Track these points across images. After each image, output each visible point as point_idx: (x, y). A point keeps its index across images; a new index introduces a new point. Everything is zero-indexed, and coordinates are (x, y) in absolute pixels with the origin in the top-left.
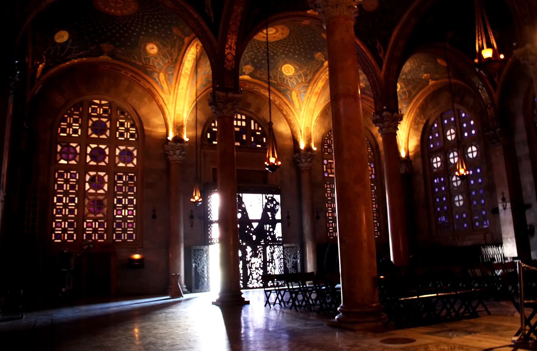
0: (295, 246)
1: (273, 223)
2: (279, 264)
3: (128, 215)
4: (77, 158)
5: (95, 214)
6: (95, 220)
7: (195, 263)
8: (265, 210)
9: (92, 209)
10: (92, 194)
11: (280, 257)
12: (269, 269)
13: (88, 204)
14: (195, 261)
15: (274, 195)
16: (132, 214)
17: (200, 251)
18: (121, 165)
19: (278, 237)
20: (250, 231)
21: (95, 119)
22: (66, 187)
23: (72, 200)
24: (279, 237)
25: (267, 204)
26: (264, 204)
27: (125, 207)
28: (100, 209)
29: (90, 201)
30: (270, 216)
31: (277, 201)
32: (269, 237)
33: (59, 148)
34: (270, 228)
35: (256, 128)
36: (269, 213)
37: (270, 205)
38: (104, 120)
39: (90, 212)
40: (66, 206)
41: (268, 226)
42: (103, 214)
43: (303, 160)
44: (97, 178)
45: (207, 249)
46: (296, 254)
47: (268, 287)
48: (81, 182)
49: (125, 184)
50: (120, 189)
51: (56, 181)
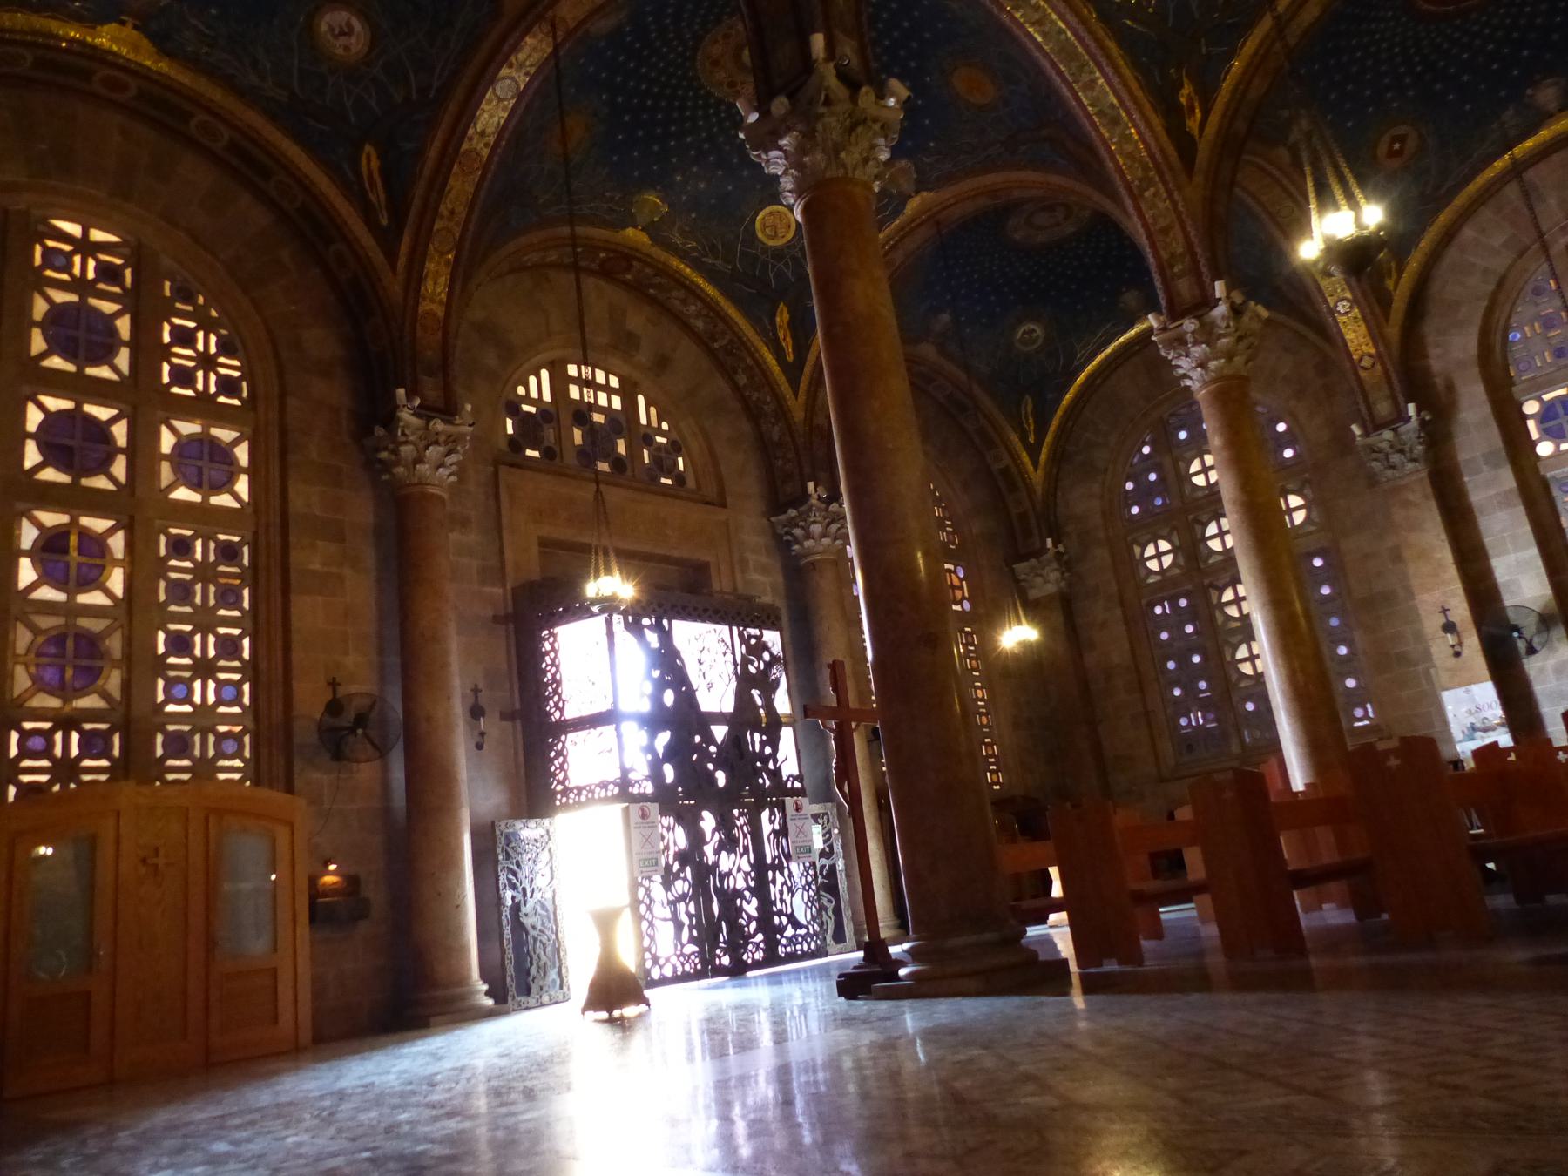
1: (773, 727)
2: (802, 874)
6: (67, 723)
7: (514, 887)
10: (48, 607)
12: (774, 891)
13: (28, 650)
14: (509, 880)
15: (765, 632)
16: (237, 701)
18: (183, 494)
20: (706, 756)
21: (60, 297)
25: (746, 662)
27: (204, 669)
28: (90, 678)
29: (41, 639)
30: (759, 702)
34: (763, 744)
35: (654, 424)
36: (755, 693)
37: (756, 664)
39: (39, 685)
41: (757, 737)
42: (105, 696)
43: (816, 529)
44: (74, 540)
45: (548, 831)
49: (204, 572)
50: (181, 592)
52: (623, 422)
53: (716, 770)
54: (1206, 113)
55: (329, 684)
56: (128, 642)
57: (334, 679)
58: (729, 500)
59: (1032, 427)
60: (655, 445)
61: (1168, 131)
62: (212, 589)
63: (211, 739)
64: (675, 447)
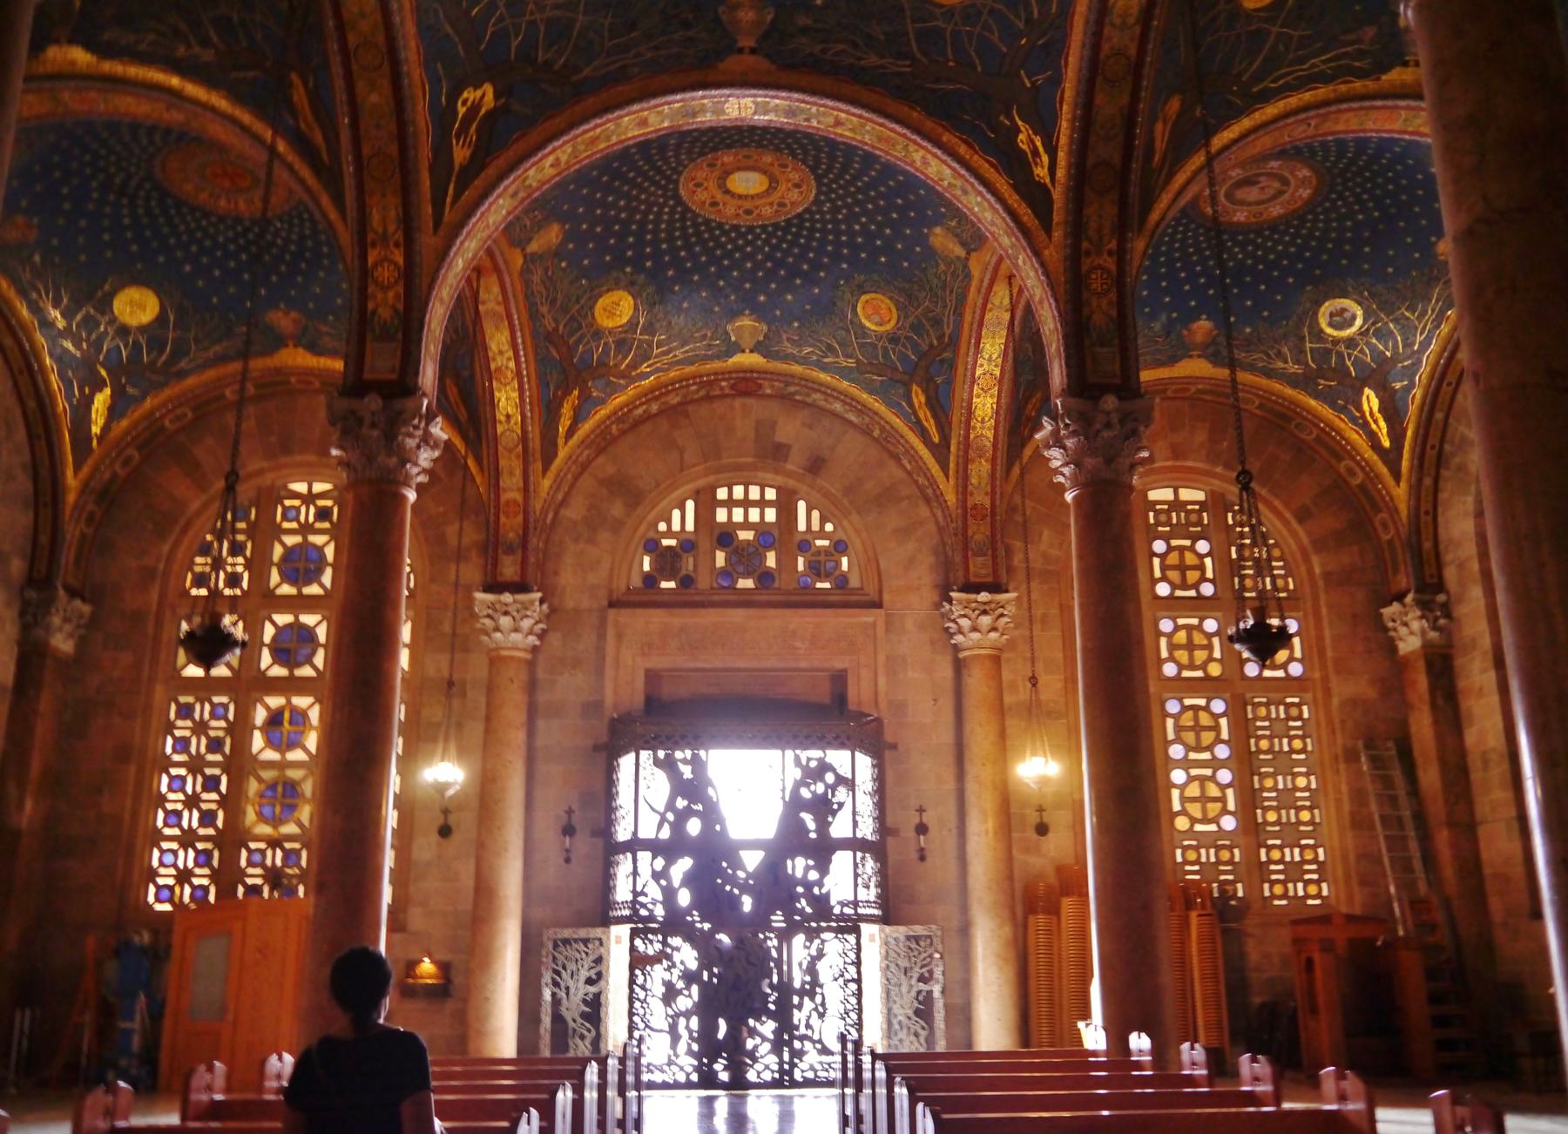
0: (926, 933)
1: (822, 851)
5: (276, 822)
8: (795, 805)
9: (267, 811)
10: (270, 765)
11: (842, 976)
12: (798, 1017)
15: (828, 752)
17: (575, 946)
19: (839, 903)
20: (733, 881)
21: (291, 540)
24: (843, 904)
25: (798, 784)
26: (789, 786)
30: (811, 825)
31: (841, 772)
32: (803, 901)
34: (807, 869)
35: (816, 527)
36: (808, 819)
38: (319, 540)
39: (261, 817)
42: (300, 824)
43: (965, 623)
44: (287, 715)
46: (930, 963)
47: (794, 1084)
48: (240, 729)
51: (170, 728)
52: (781, 535)
53: (741, 894)
54: (1052, 151)
58: (886, 597)
59: (1385, 431)
60: (813, 549)
61: (1016, 188)
64: (840, 547)
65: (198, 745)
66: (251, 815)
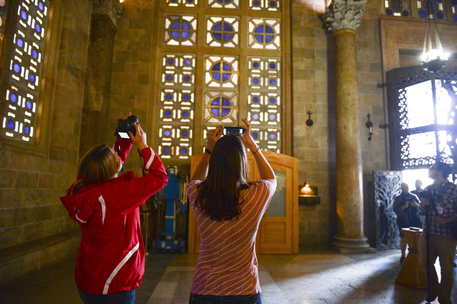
3: (269, 120)
4: (194, 38)
7: (381, 198)
13: (209, 104)
14: (380, 196)
16: (275, 120)
22: (179, 78)
23: (186, 97)
27: (264, 109)
29: (212, 100)
33: (168, 23)
40: (177, 106)
44: (222, 65)
45: (399, 177)
49: (264, 74)
51: (164, 70)
55: (308, 113)
56: (239, 100)
57: (309, 112)
62: (267, 79)
63: (266, 134)
65: (179, 78)
66: (207, 114)
